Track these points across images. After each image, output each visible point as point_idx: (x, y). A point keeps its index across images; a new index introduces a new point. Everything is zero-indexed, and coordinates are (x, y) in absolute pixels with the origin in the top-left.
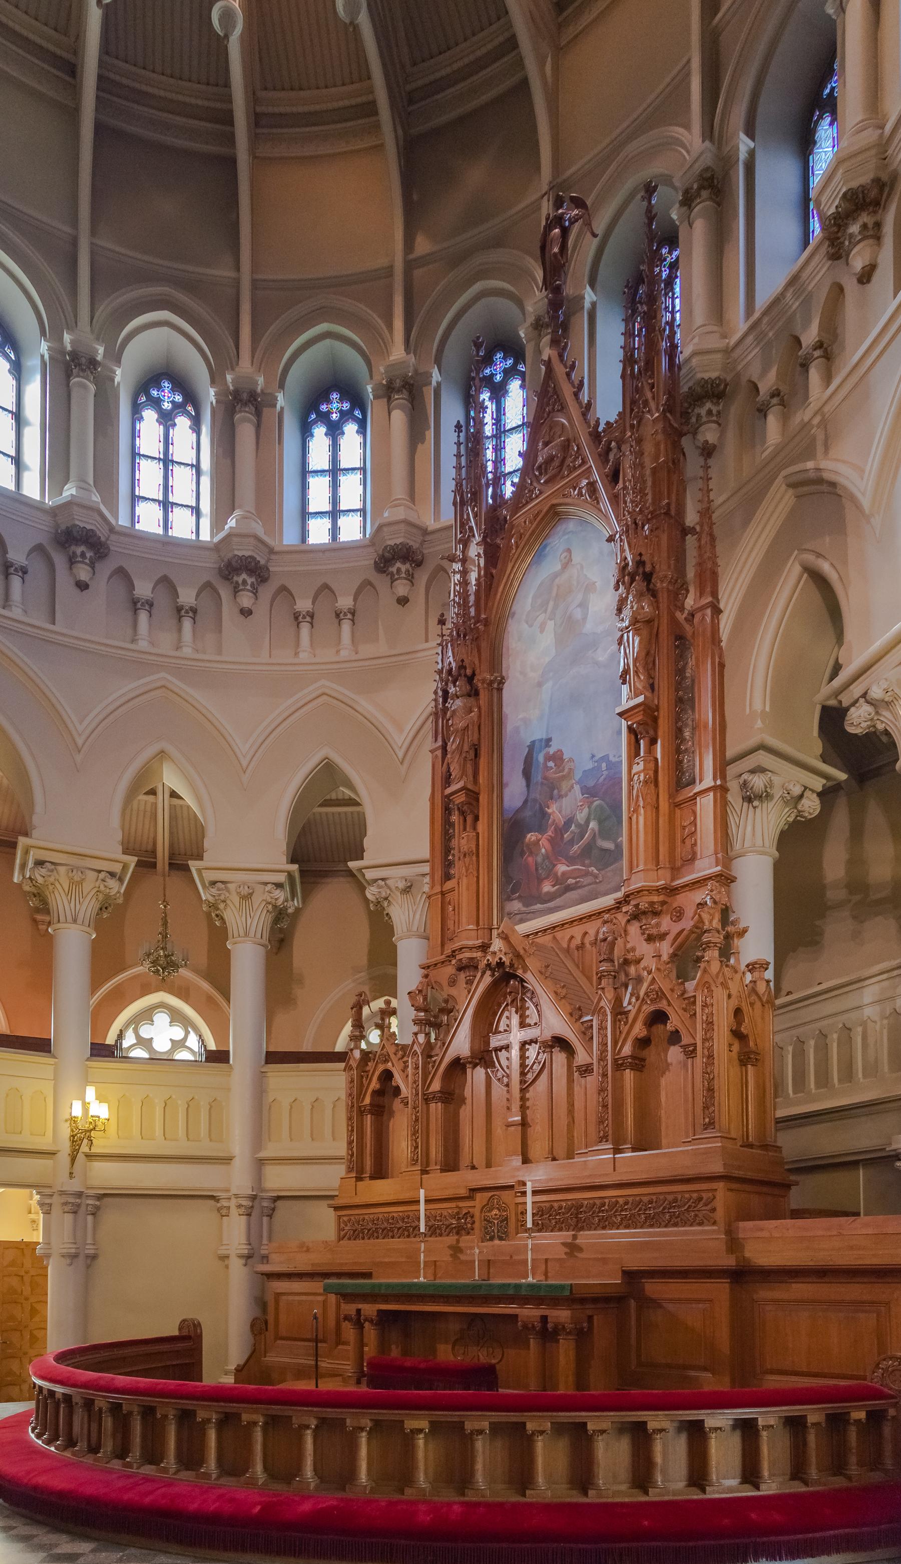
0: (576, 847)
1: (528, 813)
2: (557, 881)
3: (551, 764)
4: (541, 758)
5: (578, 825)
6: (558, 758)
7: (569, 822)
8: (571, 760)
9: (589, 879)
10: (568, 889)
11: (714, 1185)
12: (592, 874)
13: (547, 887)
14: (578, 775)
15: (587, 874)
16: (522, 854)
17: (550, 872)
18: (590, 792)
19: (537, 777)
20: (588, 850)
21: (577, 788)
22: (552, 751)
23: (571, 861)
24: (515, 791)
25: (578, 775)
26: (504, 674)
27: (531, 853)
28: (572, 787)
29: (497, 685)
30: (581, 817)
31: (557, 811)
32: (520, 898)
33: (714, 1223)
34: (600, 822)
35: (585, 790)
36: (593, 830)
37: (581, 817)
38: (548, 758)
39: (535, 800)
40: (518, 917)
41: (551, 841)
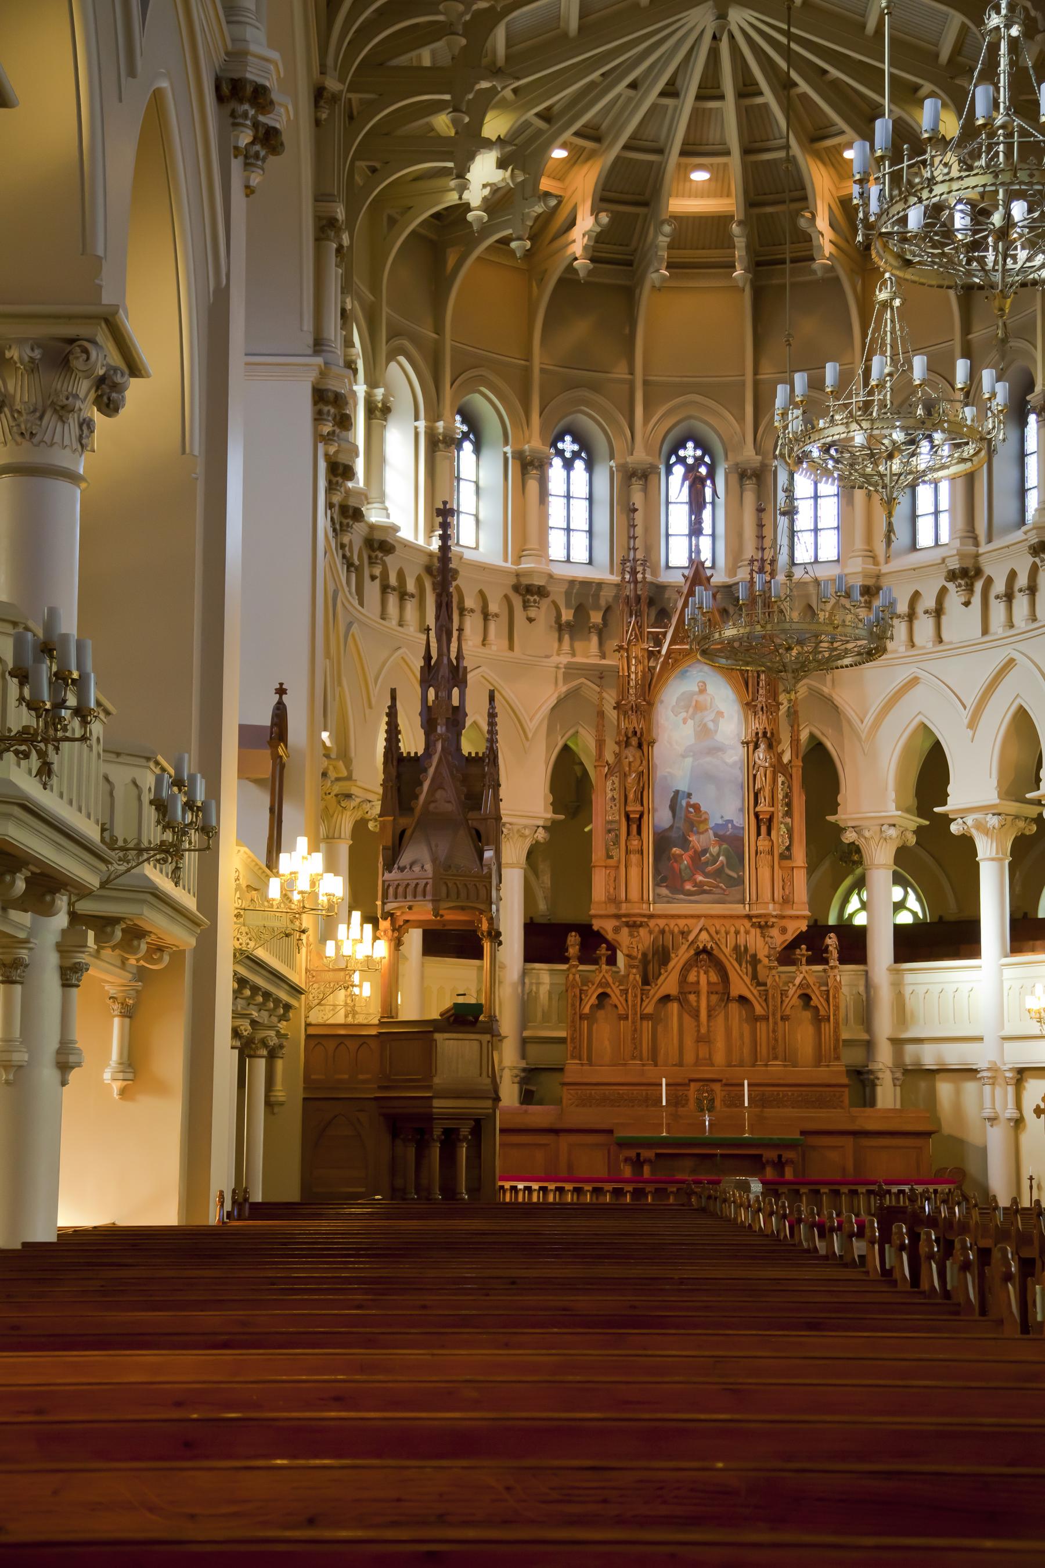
0: (710, 868)
1: (673, 834)
2: (696, 884)
3: (691, 810)
4: (684, 803)
5: (711, 855)
6: (697, 807)
7: (705, 851)
8: (706, 813)
9: (720, 891)
10: (705, 892)
11: (843, 1089)
12: (721, 888)
13: (688, 886)
14: (711, 824)
15: (717, 887)
16: (669, 859)
17: (691, 879)
18: (721, 838)
19: (681, 814)
20: (719, 873)
21: (711, 832)
22: (692, 802)
23: (706, 875)
24: (661, 817)
25: (711, 824)
26: (654, 736)
27: (676, 861)
28: (707, 830)
29: (652, 743)
30: (714, 850)
31: (697, 841)
32: (666, 887)
33: (842, 1108)
34: (728, 858)
35: (716, 835)
36: (722, 862)
37: (714, 850)
38: (689, 805)
39: (679, 828)
40: (666, 899)
41: (692, 858)
